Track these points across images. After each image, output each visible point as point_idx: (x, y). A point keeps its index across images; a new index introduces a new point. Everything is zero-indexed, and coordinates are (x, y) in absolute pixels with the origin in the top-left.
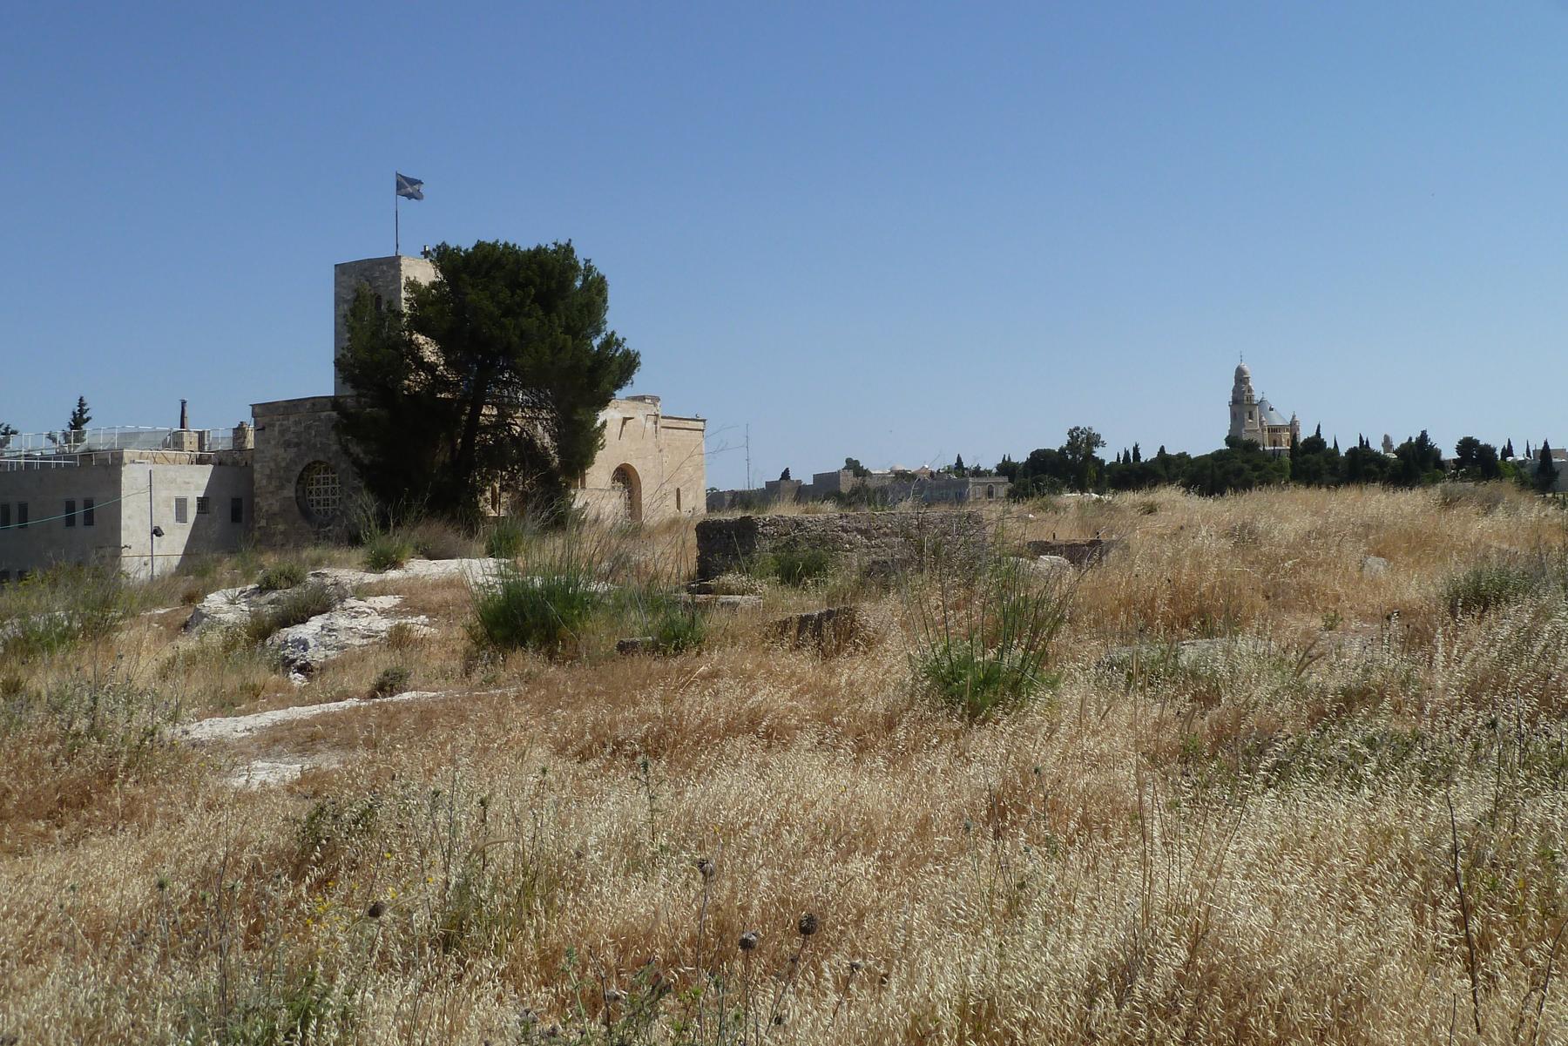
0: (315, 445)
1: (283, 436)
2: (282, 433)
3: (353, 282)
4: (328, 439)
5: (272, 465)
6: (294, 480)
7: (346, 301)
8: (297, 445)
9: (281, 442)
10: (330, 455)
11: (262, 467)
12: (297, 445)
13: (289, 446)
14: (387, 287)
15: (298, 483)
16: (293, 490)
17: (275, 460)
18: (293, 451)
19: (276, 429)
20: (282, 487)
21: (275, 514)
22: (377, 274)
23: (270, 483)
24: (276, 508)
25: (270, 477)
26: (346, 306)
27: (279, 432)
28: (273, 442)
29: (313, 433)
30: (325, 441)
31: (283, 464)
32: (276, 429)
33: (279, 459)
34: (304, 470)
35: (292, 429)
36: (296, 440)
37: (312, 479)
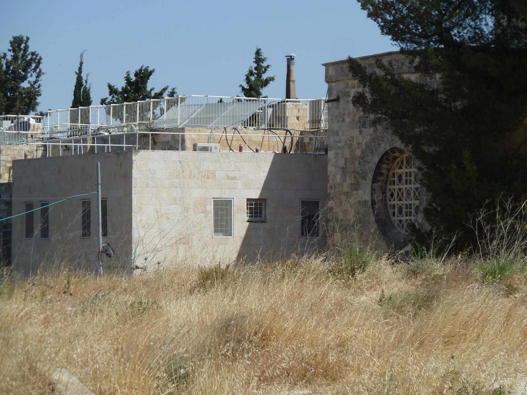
5: (347, 152)
6: (370, 176)
17: (350, 146)
20: (356, 187)
33: (354, 145)
34: (381, 161)
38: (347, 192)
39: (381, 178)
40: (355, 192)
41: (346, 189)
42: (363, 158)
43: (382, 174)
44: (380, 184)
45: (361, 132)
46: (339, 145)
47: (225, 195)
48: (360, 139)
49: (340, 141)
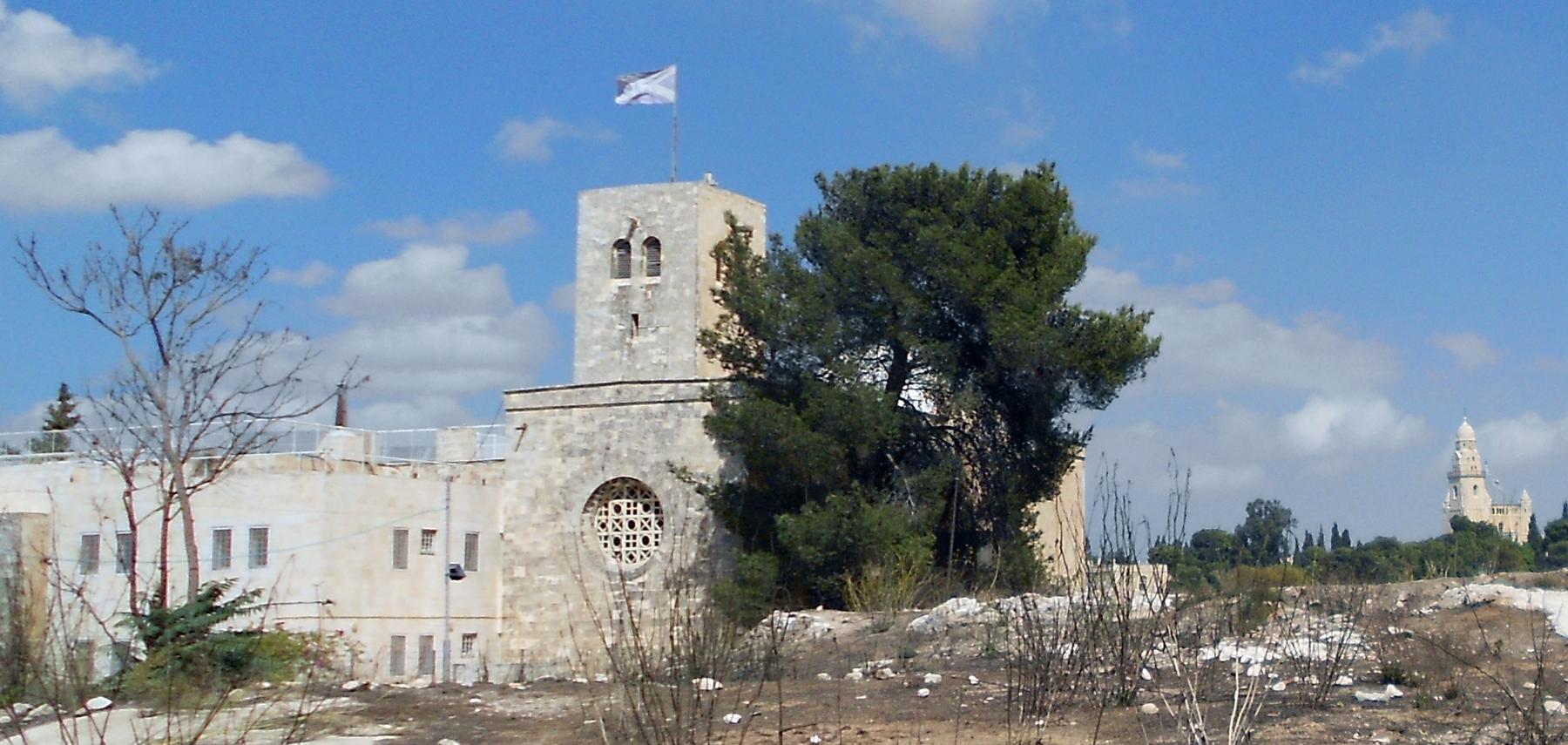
0: (618, 455)
1: (560, 438)
2: (559, 434)
3: (612, 217)
4: (641, 443)
5: (539, 483)
7: (601, 247)
8: (585, 452)
9: (558, 446)
10: (646, 469)
11: (521, 486)
12: (585, 452)
13: (570, 454)
14: (672, 228)
15: (585, 511)
16: (576, 521)
17: (545, 476)
18: (577, 463)
19: (548, 428)
20: (556, 516)
21: (542, 559)
22: (655, 209)
23: (534, 511)
24: (544, 549)
25: (534, 502)
26: (598, 255)
27: (554, 432)
28: (541, 448)
29: (616, 438)
30: (635, 446)
31: (559, 482)
32: (548, 428)
34: (596, 492)
35: (577, 429)
36: (584, 446)
37: (606, 506)
38: (539, 524)
39: (590, 509)
40: (552, 524)
41: (535, 519)
42: (567, 488)
43: (593, 505)
44: (589, 515)
45: (564, 461)
46: (526, 474)
47: (401, 525)
48: (563, 468)
49: (527, 471)
